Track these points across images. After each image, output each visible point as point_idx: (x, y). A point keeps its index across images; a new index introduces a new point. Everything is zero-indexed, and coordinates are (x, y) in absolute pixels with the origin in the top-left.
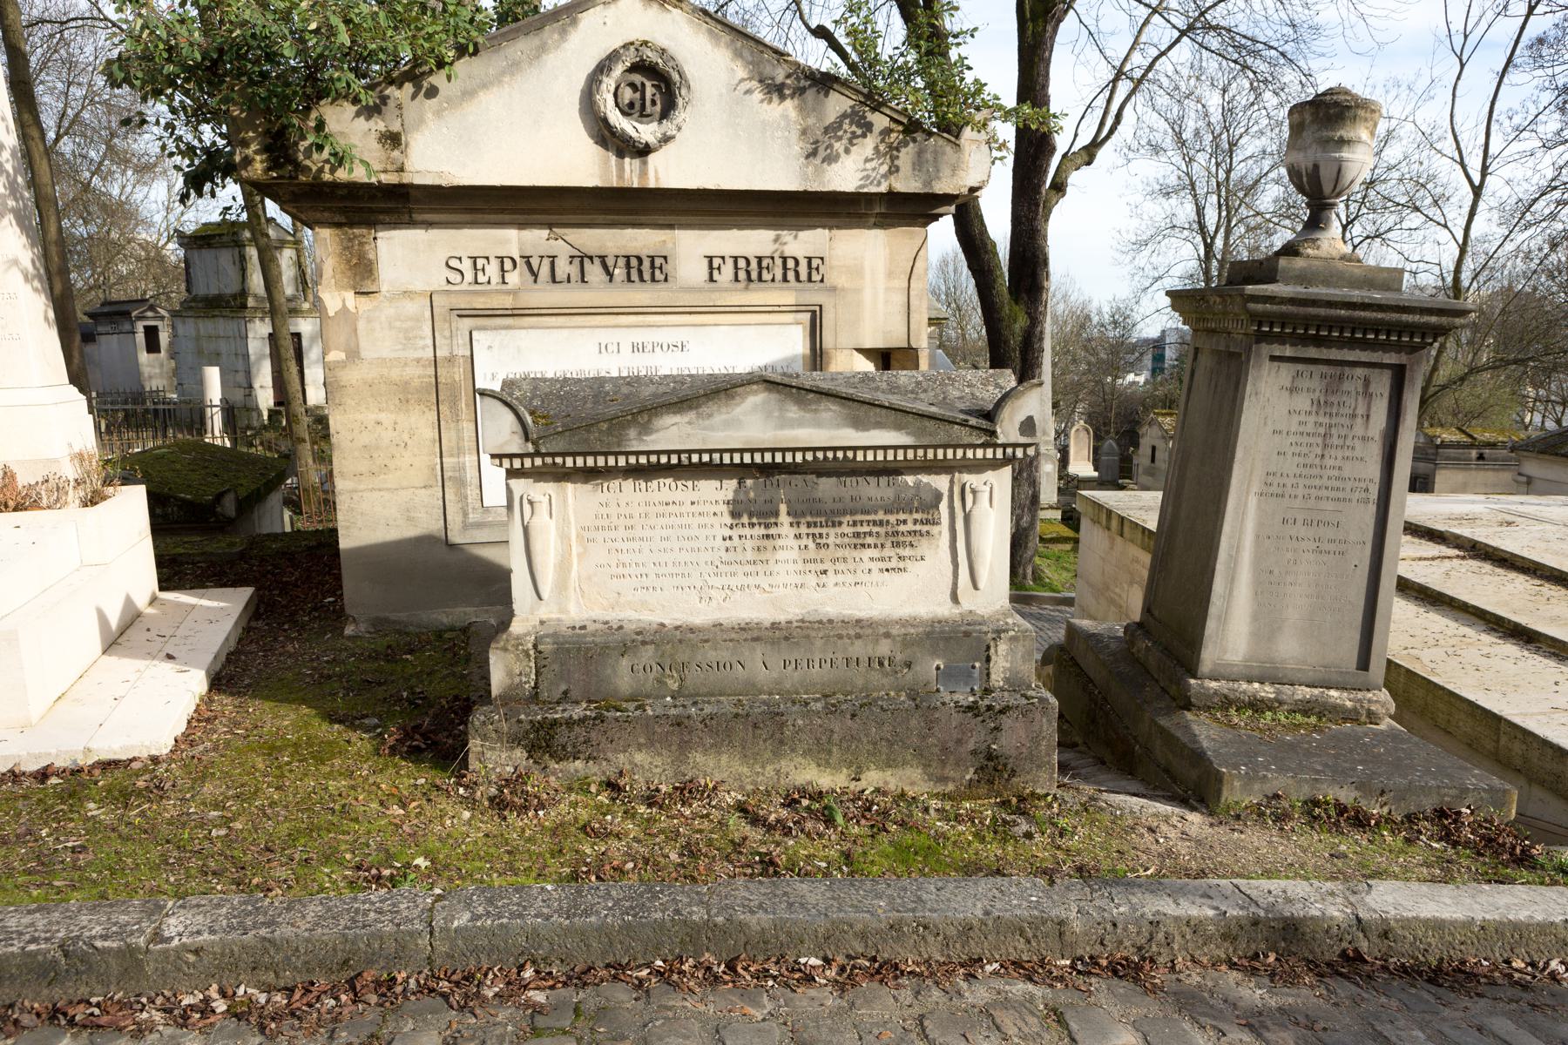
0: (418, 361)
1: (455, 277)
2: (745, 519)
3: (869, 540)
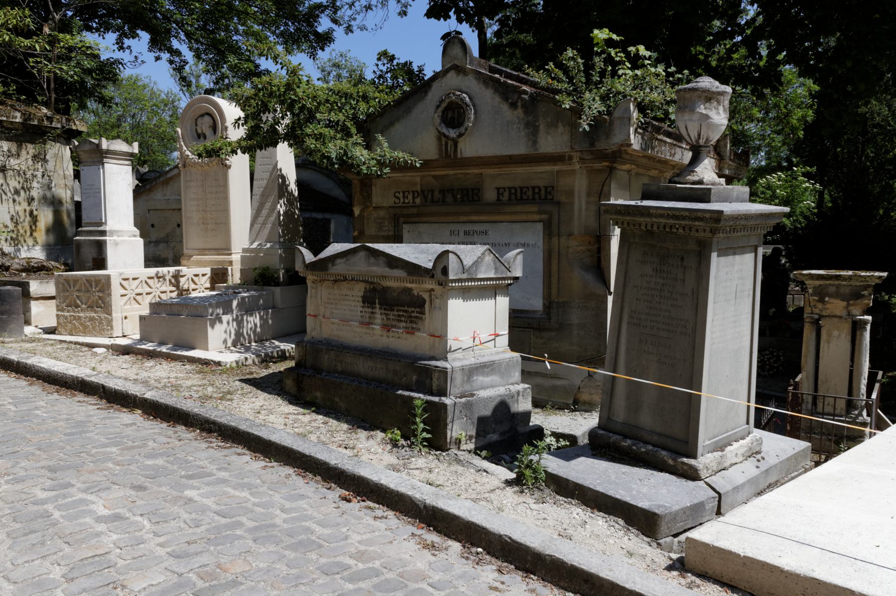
0: (383, 236)
1: (397, 201)
2: (366, 305)
3: (403, 319)
